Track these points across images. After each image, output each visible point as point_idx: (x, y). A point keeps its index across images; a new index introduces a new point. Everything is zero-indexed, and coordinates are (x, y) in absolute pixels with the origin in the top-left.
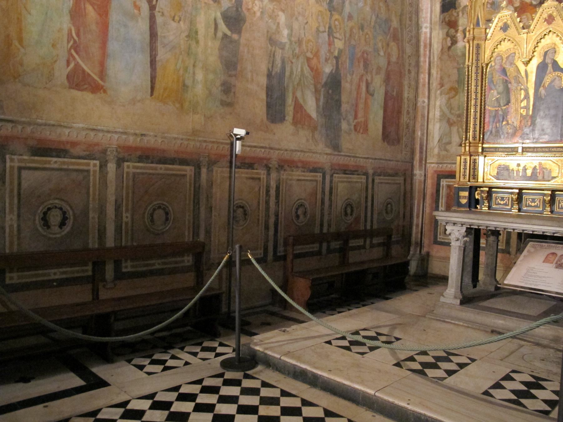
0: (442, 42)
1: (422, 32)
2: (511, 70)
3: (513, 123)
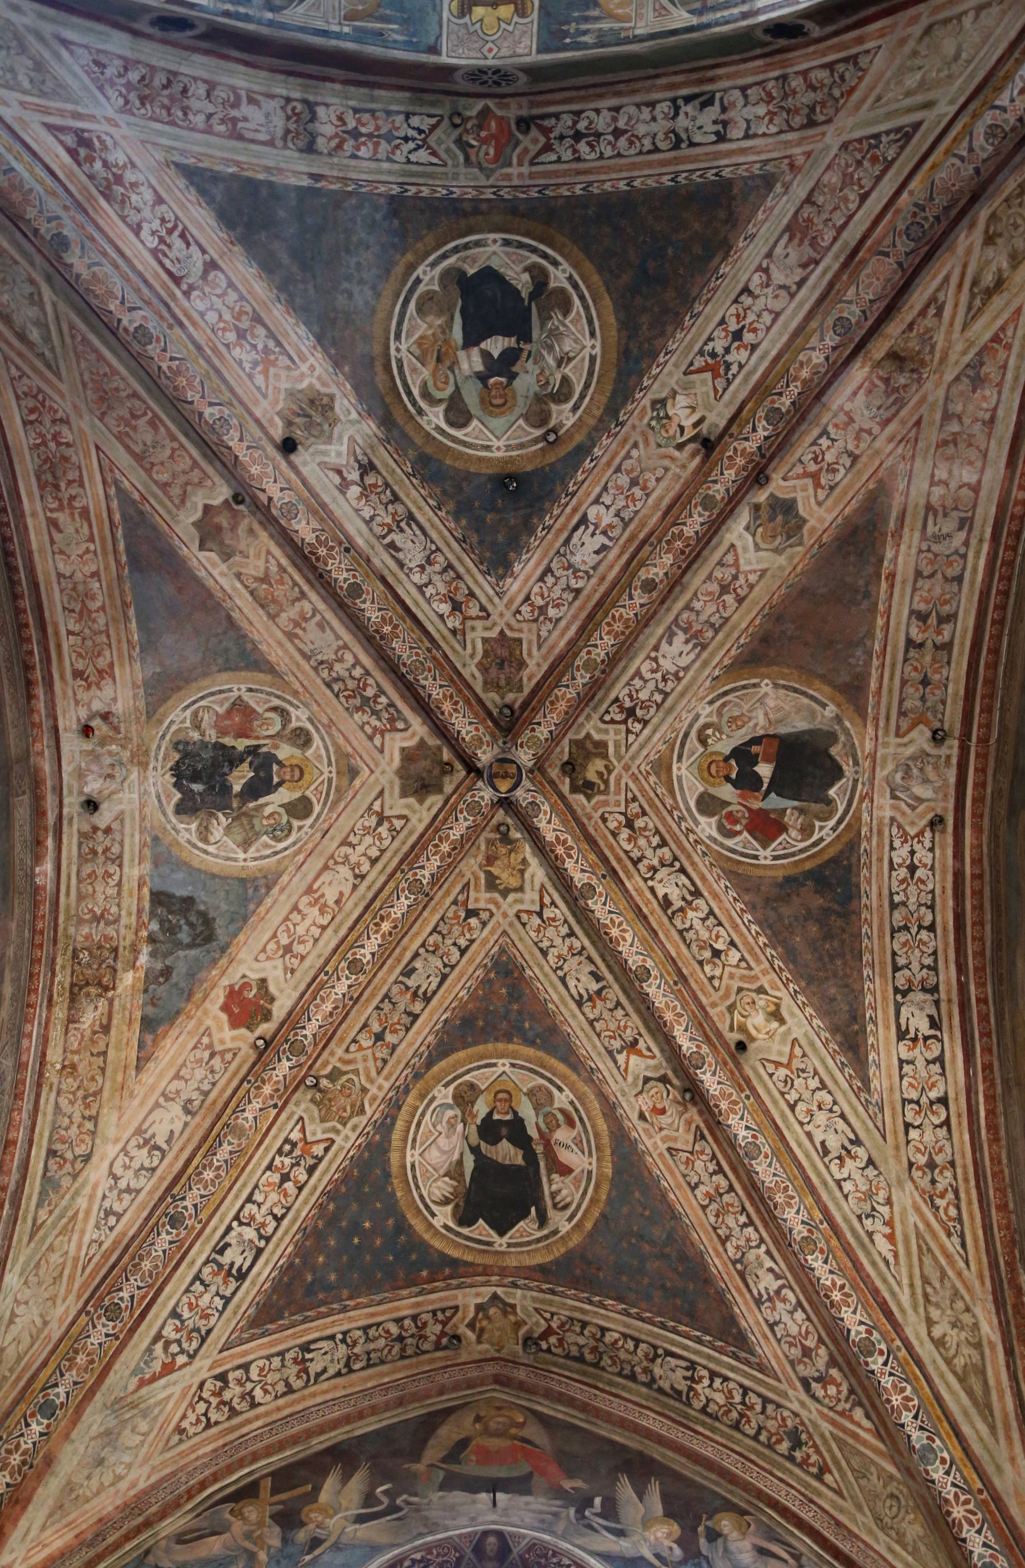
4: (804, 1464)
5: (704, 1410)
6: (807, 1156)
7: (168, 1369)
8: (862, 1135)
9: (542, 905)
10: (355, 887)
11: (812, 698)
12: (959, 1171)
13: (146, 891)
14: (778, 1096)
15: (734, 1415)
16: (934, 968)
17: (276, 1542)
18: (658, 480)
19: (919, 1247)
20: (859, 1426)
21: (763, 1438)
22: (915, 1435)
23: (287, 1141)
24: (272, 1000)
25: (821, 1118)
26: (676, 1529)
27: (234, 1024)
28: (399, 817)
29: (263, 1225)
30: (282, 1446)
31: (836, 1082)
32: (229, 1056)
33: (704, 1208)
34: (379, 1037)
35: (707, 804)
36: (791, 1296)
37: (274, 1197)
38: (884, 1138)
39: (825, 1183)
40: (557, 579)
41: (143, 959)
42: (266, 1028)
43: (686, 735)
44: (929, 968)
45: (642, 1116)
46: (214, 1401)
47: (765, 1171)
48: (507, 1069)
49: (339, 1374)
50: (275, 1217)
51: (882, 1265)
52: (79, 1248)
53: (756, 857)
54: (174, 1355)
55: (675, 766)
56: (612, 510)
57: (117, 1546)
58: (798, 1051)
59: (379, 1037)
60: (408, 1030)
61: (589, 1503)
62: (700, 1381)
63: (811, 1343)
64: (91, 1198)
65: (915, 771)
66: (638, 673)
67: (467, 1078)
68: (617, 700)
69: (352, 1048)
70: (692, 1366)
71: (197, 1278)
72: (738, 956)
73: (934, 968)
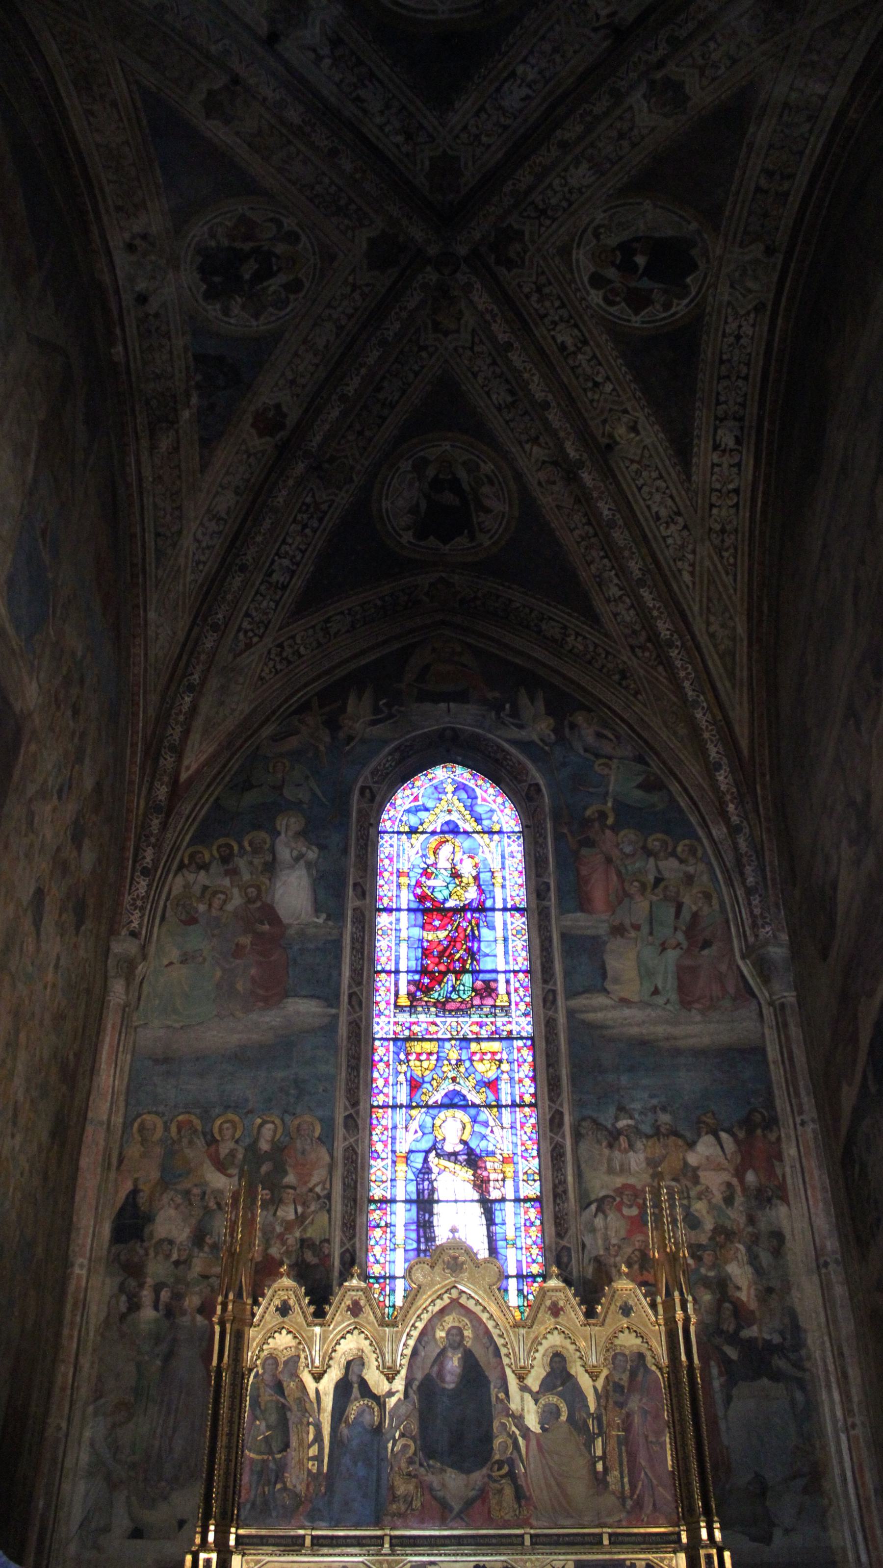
0: (109, 1303)
1: (72, 1273)
2: (291, 1386)
3: (295, 1486)
4: (627, 688)
5: (570, 651)
6: (646, 520)
7: (249, 646)
8: (682, 508)
9: (473, 343)
10: (338, 335)
11: (681, 216)
12: (740, 535)
13: (190, 354)
14: (630, 481)
15: (588, 657)
16: (743, 405)
17: (327, 739)
18: (575, 52)
19: (709, 581)
20: (660, 674)
21: (605, 670)
22: (690, 693)
23: (304, 503)
24: (285, 416)
25: (657, 497)
26: (552, 721)
27: (261, 435)
28: (367, 285)
29: (294, 556)
30: (319, 677)
31: (669, 474)
32: (260, 455)
33: (578, 543)
34: (360, 433)
35: (597, 281)
36: (628, 600)
37: (299, 539)
38: (696, 512)
39: (655, 537)
40: (489, 115)
41: (194, 400)
42: (282, 434)
43: (584, 231)
44: (740, 404)
45: (540, 483)
46: (278, 659)
47: (619, 536)
48: (448, 448)
49: (348, 631)
50: (301, 550)
51: (684, 588)
52: (184, 585)
53: (629, 321)
54: (251, 638)
55: (574, 252)
56: (536, 69)
57: (241, 747)
58: (646, 453)
59: (360, 433)
60: (380, 426)
61: (504, 709)
62: (569, 636)
63: (637, 627)
64: (186, 557)
65: (750, 272)
66: (550, 185)
67: (422, 454)
68: (533, 203)
69: (343, 442)
70: (565, 627)
71: (257, 592)
72: (611, 387)
73: (743, 405)
